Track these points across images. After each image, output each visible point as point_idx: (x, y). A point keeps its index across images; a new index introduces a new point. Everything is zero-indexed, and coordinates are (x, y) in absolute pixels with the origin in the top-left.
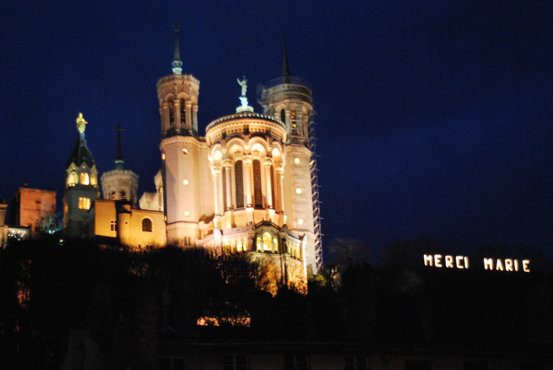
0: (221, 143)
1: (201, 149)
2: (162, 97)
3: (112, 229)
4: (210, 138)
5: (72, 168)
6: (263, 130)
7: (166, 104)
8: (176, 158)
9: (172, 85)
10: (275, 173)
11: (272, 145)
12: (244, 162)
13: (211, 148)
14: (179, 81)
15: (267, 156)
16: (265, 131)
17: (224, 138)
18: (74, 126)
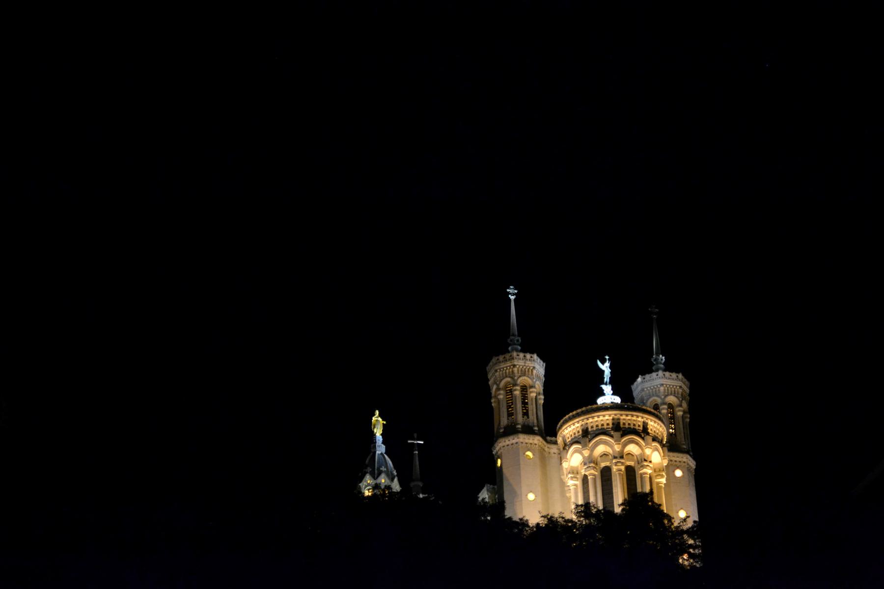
0: (582, 443)
1: (549, 453)
2: (495, 383)
4: (564, 437)
5: (366, 481)
6: (639, 426)
7: (502, 392)
8: (517, 464)
9: (510, 366)
11: (652, 446)
12: (614, 469)
13: (565, 451)
14: (519, 361)
17: (586, 435)
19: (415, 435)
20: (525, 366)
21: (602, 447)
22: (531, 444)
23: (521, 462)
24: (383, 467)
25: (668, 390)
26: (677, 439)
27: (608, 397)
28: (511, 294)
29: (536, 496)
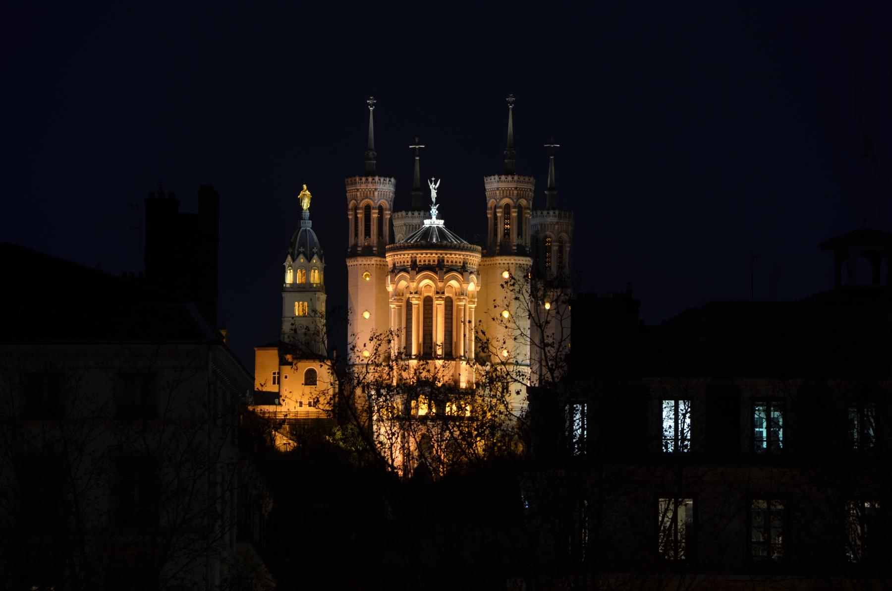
3: (274, 383)
10: (454, 309)
15: (438, 293)
16: (436, 263)
18: (298, 203)
19: (417, 140)
20: (367, 189)
22: (369, 265)
23: (359, 284)
24: (302, 248)
25: (503, 192)
26: (509, 239)
28: (370, 105)
29: (371, 314)
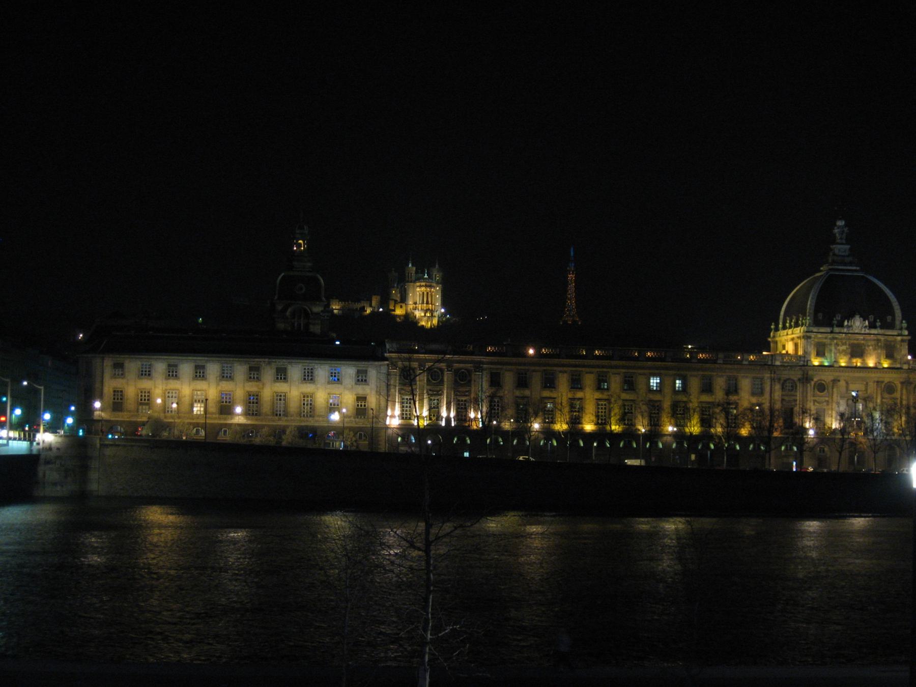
17: (420, 286)
21: (423, 289)
27: (426, 276)
